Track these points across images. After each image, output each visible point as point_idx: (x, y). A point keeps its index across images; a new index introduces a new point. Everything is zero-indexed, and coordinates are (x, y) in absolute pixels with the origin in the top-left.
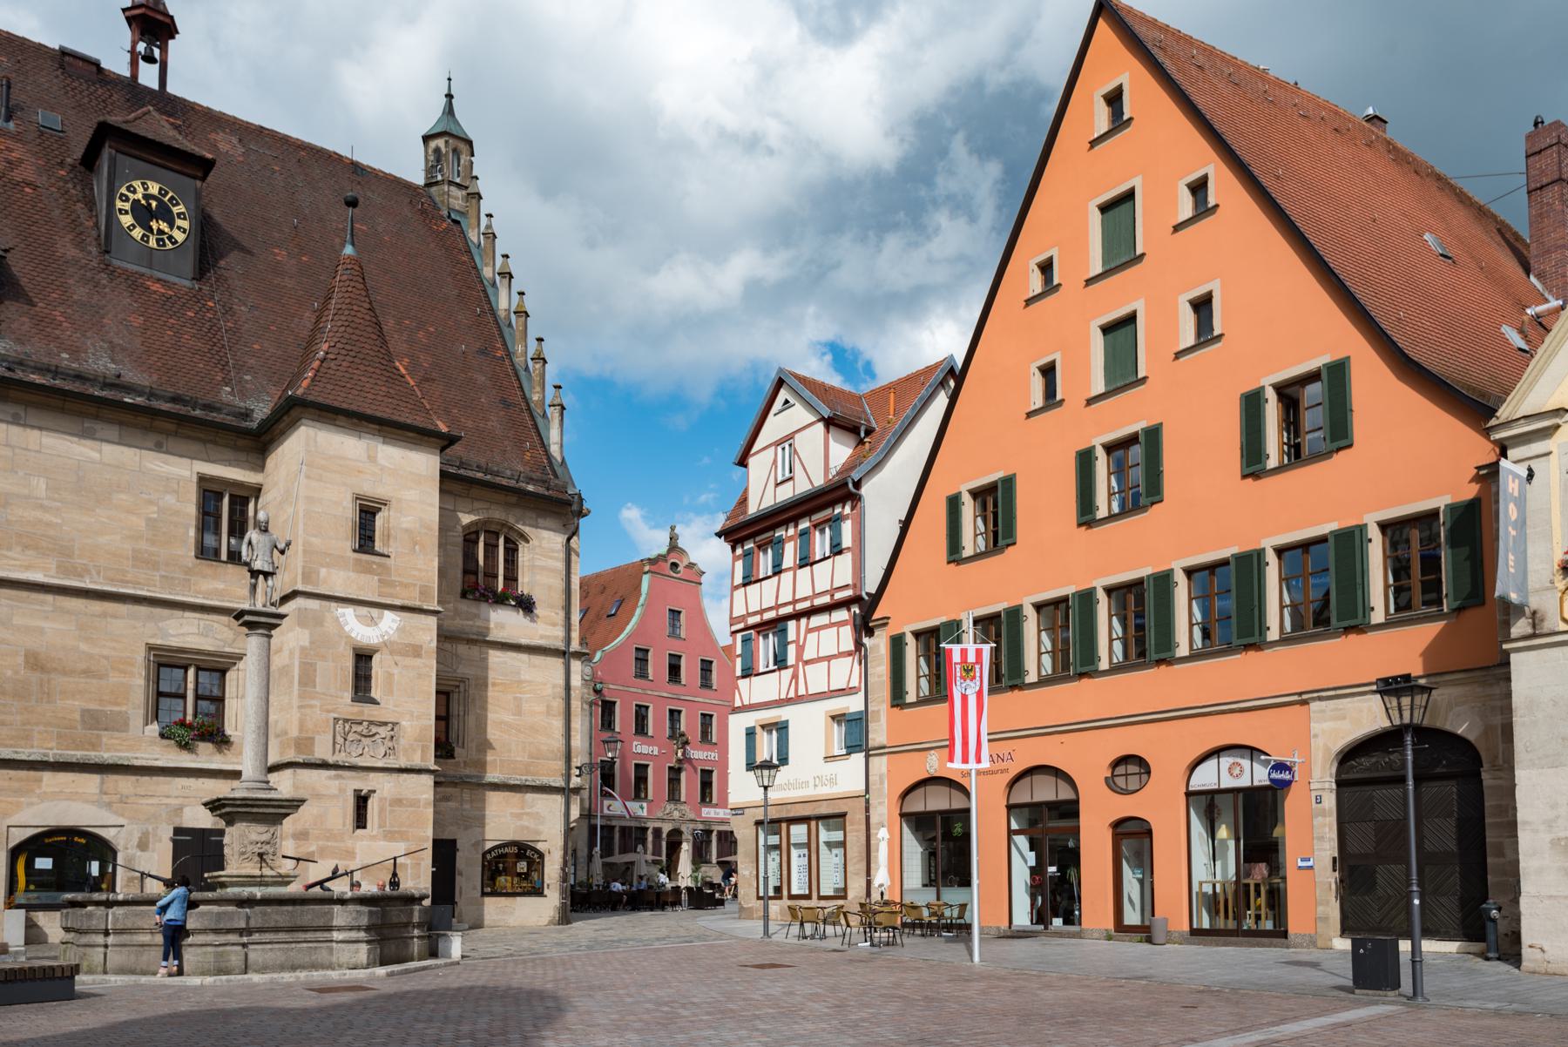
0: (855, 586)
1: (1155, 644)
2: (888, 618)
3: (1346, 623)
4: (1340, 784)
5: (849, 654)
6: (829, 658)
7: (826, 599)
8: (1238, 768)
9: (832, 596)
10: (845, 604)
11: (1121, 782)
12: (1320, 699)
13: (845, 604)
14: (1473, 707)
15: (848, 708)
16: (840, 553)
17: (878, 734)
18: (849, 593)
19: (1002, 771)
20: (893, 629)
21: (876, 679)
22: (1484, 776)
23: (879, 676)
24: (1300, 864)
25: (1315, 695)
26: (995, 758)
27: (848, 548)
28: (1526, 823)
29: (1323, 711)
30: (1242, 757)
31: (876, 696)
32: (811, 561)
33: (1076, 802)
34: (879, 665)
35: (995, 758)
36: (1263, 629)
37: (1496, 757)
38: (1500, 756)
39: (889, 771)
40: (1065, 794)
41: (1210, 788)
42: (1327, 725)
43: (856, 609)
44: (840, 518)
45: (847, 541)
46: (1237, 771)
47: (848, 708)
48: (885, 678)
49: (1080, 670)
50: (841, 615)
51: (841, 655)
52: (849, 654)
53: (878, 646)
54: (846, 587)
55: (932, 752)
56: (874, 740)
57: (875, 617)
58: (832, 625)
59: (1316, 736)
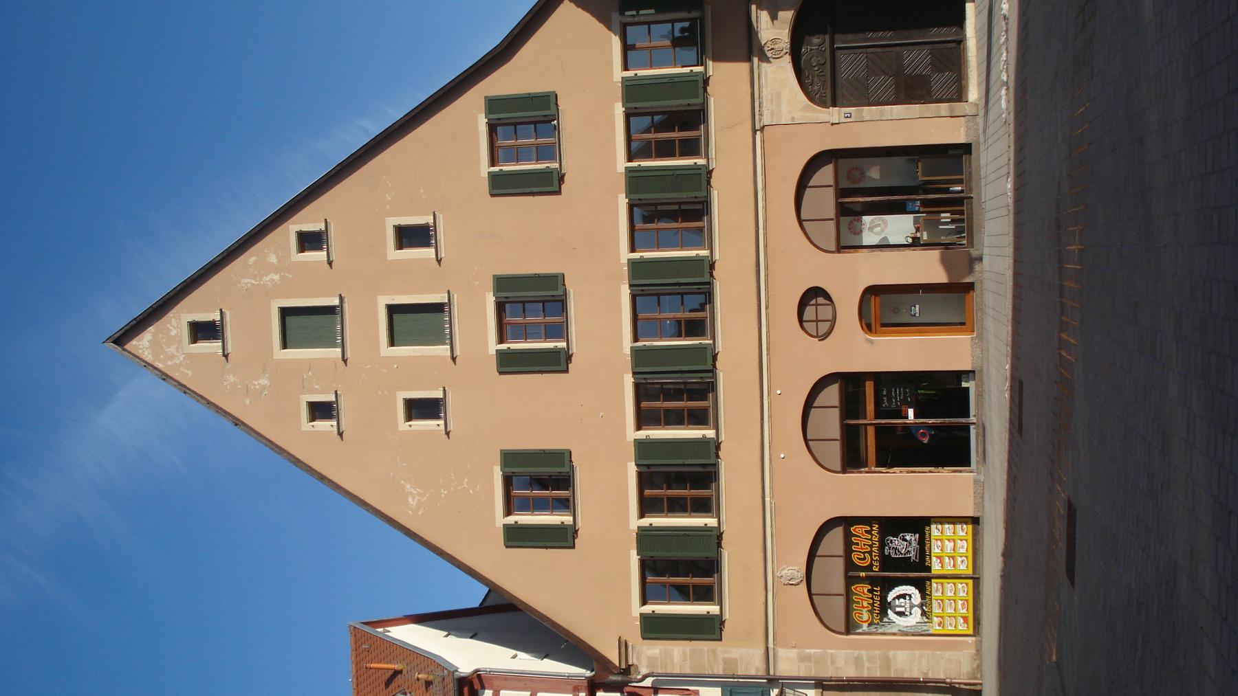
3: (701, 91)
4: (834, 105)
11: (824, 328)
12: (761, 115)
20: (633, 632)
21: (688, 662)
23: (685, 660)
25: (757, 117)
29: (772, 115)
40: (832, 395)
42: (784, 108)
56: (757, 669)
59: (793, 119)
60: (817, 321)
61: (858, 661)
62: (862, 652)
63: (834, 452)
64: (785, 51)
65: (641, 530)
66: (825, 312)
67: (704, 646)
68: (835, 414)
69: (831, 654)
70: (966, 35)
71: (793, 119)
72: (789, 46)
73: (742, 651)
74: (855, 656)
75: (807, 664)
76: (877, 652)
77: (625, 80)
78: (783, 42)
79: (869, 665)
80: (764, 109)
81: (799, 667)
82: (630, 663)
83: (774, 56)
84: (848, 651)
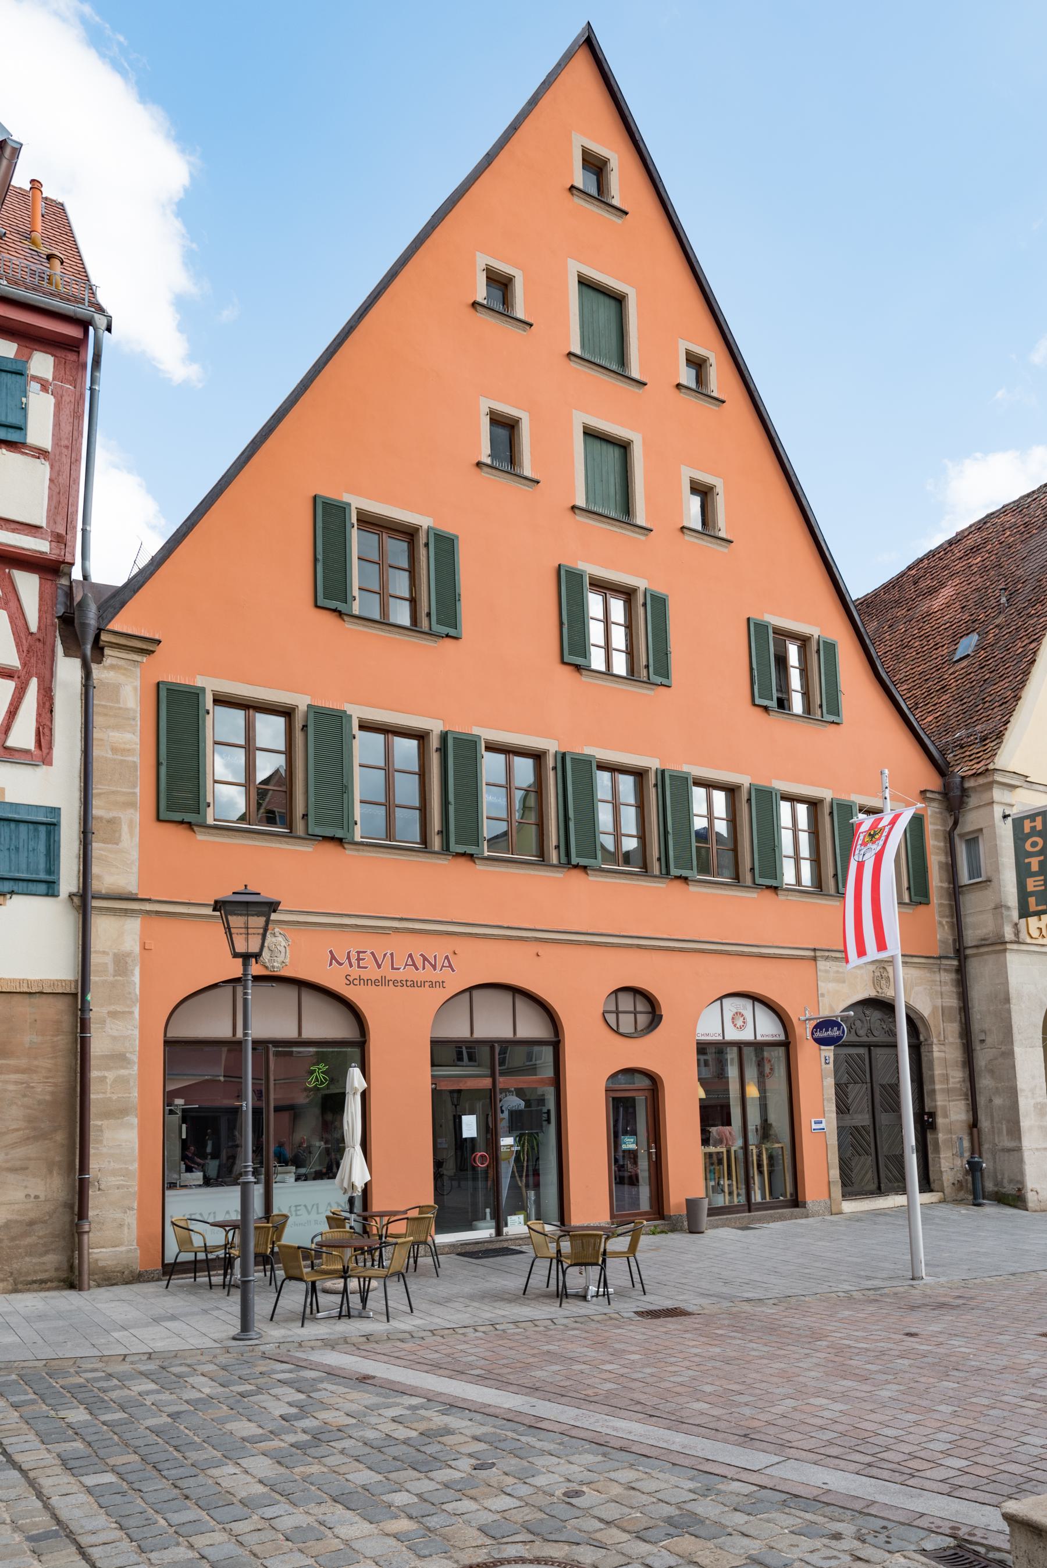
11: (611, 1018)
12: (827, 958)
19: (432, 985)
24: (814, 1126)
25: (826, 954)
26: (419, 962)
29: (827, 971)
30: (745, 1008)
35: (419, 962)
41: (714, 1038)
42: (831, 986)
46: (740, 1023)
59: (823, 995)
60: (617, 1013)
61: (119, 1059)
62: (136, 1068)
64: (880, 991)
66: (627, 1023)
68: (506, 1033)
71: (823, 995)
74: (128, 1055)
76: (135, 1094)
80: (832, 963)
84: (137, 1042)
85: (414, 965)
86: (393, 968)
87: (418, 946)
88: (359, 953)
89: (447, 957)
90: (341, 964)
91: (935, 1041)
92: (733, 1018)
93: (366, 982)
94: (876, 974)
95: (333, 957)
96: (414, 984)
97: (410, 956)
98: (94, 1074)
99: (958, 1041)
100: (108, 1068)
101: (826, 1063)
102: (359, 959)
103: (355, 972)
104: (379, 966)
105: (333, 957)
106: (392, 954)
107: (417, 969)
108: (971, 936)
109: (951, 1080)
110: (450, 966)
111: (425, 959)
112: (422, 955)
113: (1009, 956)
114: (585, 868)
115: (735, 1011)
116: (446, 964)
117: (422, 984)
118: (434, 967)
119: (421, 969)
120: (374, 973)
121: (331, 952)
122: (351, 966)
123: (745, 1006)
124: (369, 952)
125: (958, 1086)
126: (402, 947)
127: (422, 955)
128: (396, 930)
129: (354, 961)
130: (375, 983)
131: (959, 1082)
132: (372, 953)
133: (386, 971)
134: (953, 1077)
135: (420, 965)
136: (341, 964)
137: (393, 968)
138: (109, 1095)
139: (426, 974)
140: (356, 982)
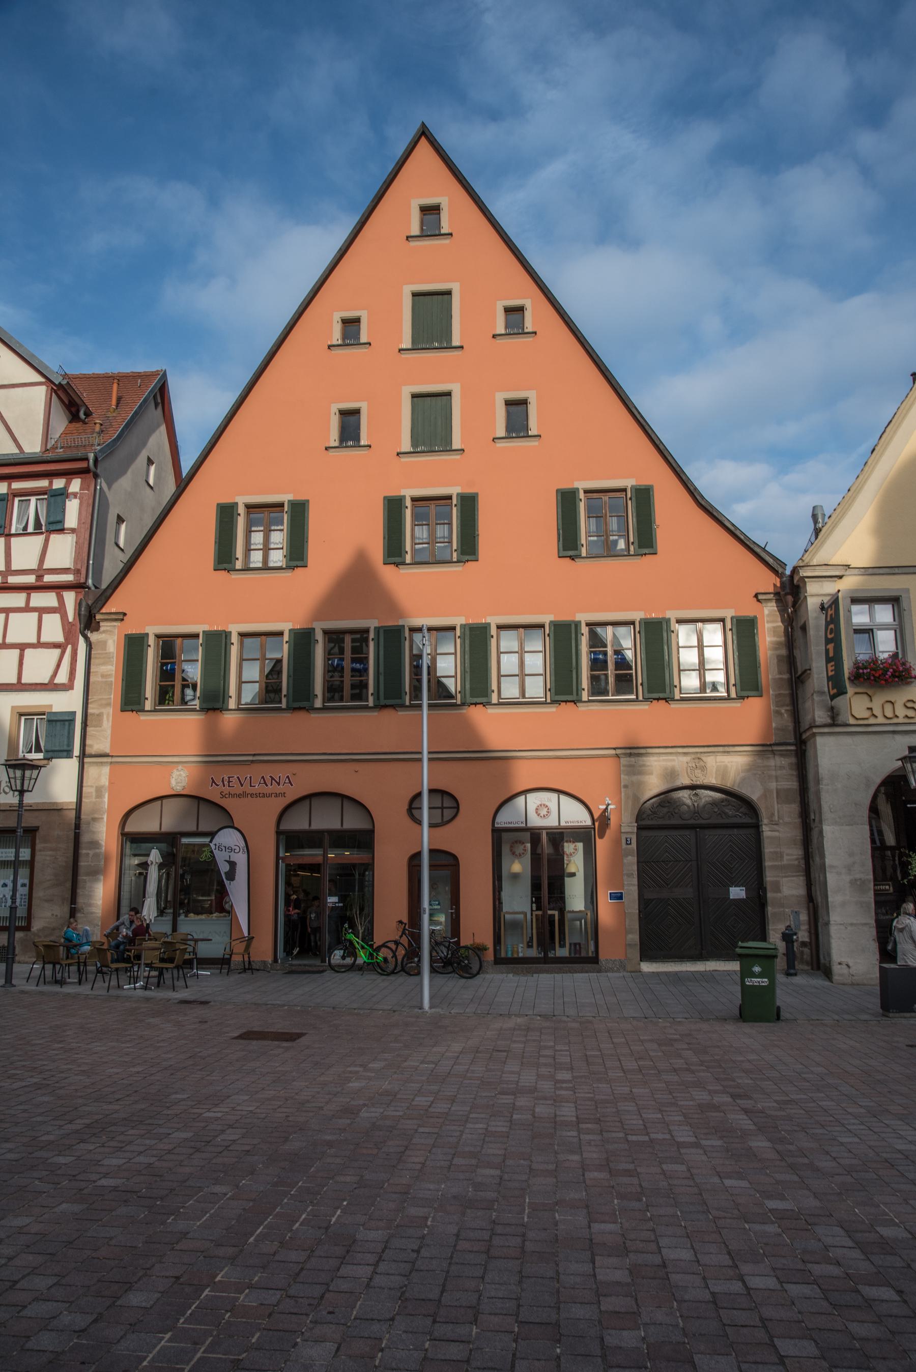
0: (77, 572)
1: (471, 688)
2: (125, 614)
4: (639, 828)
5: (55, 646)
6: (22, 647)
7: (31, 579)
8: (546, 809)
9: (40, 577)
10: (58, 588)
13: (58, 588)
14: (755, 774)
15: (51, 706)
16: (62, 530)
17: (100, 741)
18: (69, 578)
19: (277, 795)
21: (100, 679)
22: (764, 826)
23: (103, 676)
27: (73, 531)
28: (832, 867)
30: (550, 800)
31: (96, 698)
32: (6, 532)
33: (371, 832)
34: (104, 664)
36: (579, 690)
37: (773, 814)
38: (776, 814)
39: (111, 783)
40: (353, 822)
41: (517, 825)
43: (70, 598)
44: (63, 494)
45: (72, 518)
47: (51, 706)
48: (113, 679)
49: (383, 702)
50: (48, 599)
51: (39, 645)
52: (55, 646)
53: (104, 644)
54: (65, 571)
55: (180, 767)
56: (91, 746)
57: (104, 610)
58: (27, 609)
63: (298, 822)
64: (694, 779)
65: (227, 635)
67: (114, 694)
68: (336, 825)
69: (103, 818)
70: (708, 960)
72: (698, 783)
73: (109, 732)
75: (94, 794)
77: (668, 621)
78: (703, 778)
79: (90, 856)
81: (92, 786)
82: (102, 624)
83: (689, 769)
85: (265, 783)
86: (251, 786)
87: (267, 771)
88: (229, 778)
89: (288, 777)
90: (218, 785)
91: (765, 821)
92: (537, 809)
93: (233, 796)
94: (690, 765)
95: (213, 781)
96: (264, 795)
97: (263, 777)
98: (83, 851)
99: (798, 821)
100: (90, 849)
101: (627, 844)
102: (229, 782)
103: (226, 790)
104: (242, 785)
105: (213, 781)
106: (250, 777)
107: (267, 785)
108: (805, 724)
109: (786, 857)
110: (290, 782)
111: (272, 778)
112: (271, 777)
113: (819, 740)
114: (393, 706)
115: (539, 803)
116: (287, 781)
117: (270, 795)
118: (279, 784)
119: (269, 785)
120: (240, 790)
121: (212, 778)
122: (224, 786)
123: (550, 799)
124: (236, 777)
125: (796, 862)
126: (257, 772)
127: (271, 777)
128: (252, 762)
129: (226, 783)
130: (239, 796)
131: (797, 859)
132: (238, 778)
133: (247, 788)
134: (788, 855)
135: (269, 783)
136: (218, 785)
137: (251, 786)
138: (90, 863)
139: (272, 788)
140: (227, 796)
